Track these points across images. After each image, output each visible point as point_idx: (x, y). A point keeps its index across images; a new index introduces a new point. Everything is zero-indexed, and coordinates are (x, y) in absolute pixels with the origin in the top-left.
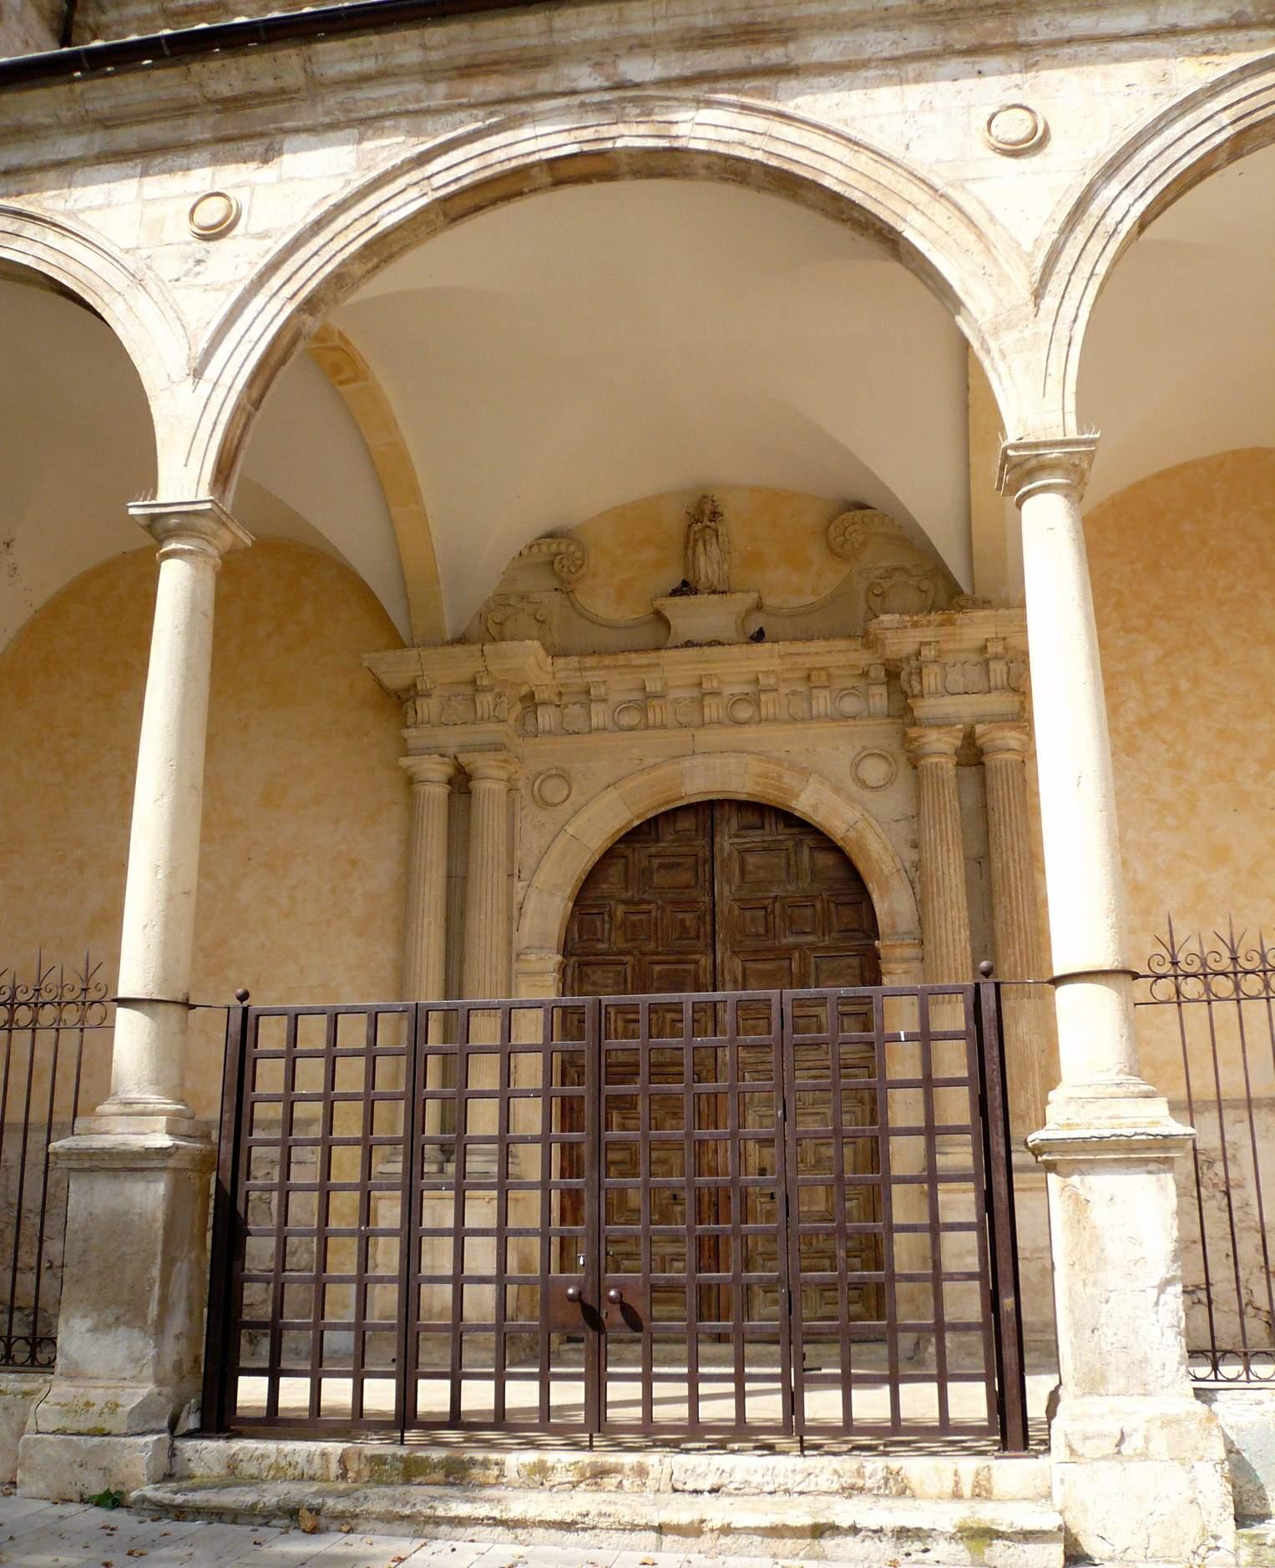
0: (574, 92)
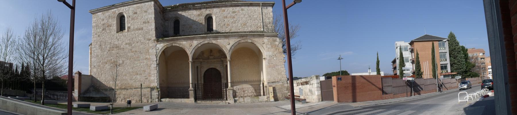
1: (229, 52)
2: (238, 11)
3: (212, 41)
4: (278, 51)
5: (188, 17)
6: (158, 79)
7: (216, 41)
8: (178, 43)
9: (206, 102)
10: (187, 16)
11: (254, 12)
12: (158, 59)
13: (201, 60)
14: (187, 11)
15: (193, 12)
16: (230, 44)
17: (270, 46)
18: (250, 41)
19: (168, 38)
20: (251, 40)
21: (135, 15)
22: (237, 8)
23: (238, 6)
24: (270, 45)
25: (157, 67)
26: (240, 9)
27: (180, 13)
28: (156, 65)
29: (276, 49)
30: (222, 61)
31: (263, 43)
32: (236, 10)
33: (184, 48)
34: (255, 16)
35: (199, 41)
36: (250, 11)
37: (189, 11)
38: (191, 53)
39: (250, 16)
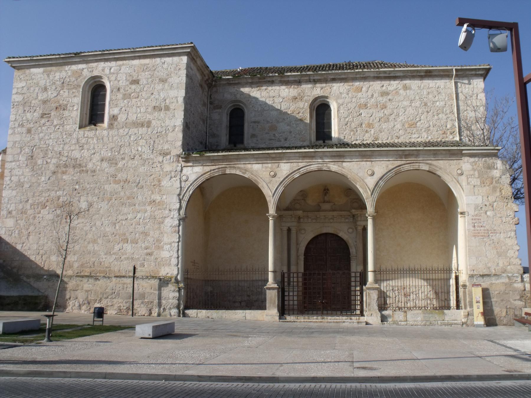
1: (372, 194)
2: (394, 92)
3: (328, 165)
4: (498, 194)
5: (266, 104)
6: (180, 259)
7: (339, 166)
8: (239, 168)
9: (309, 319)
10: (263, 99)
11: (435, 93)
12: (184, 204)
13: (300, 213)
14: (264, 88)
15: (280, 90)
16: (375, 175)
17: (479, 180)
18: (425, 167)
19: (216, 154)
20: (428, 164)
22: (392, 82)
23: (395, 78)
24: (478, 178)
25: (181, 228)
26: (400, 86)
27: (246, 90)
28: (177, 222)
29: (494, 189)
30: (354, 216)
31: (459, 172)
32: (390, 88)
33: (255, 180)
34: (438, 103)
35: (295, 164)
36: (425, 91)
37: (270, 88)
38: (273, 197)
39: (426, 104)
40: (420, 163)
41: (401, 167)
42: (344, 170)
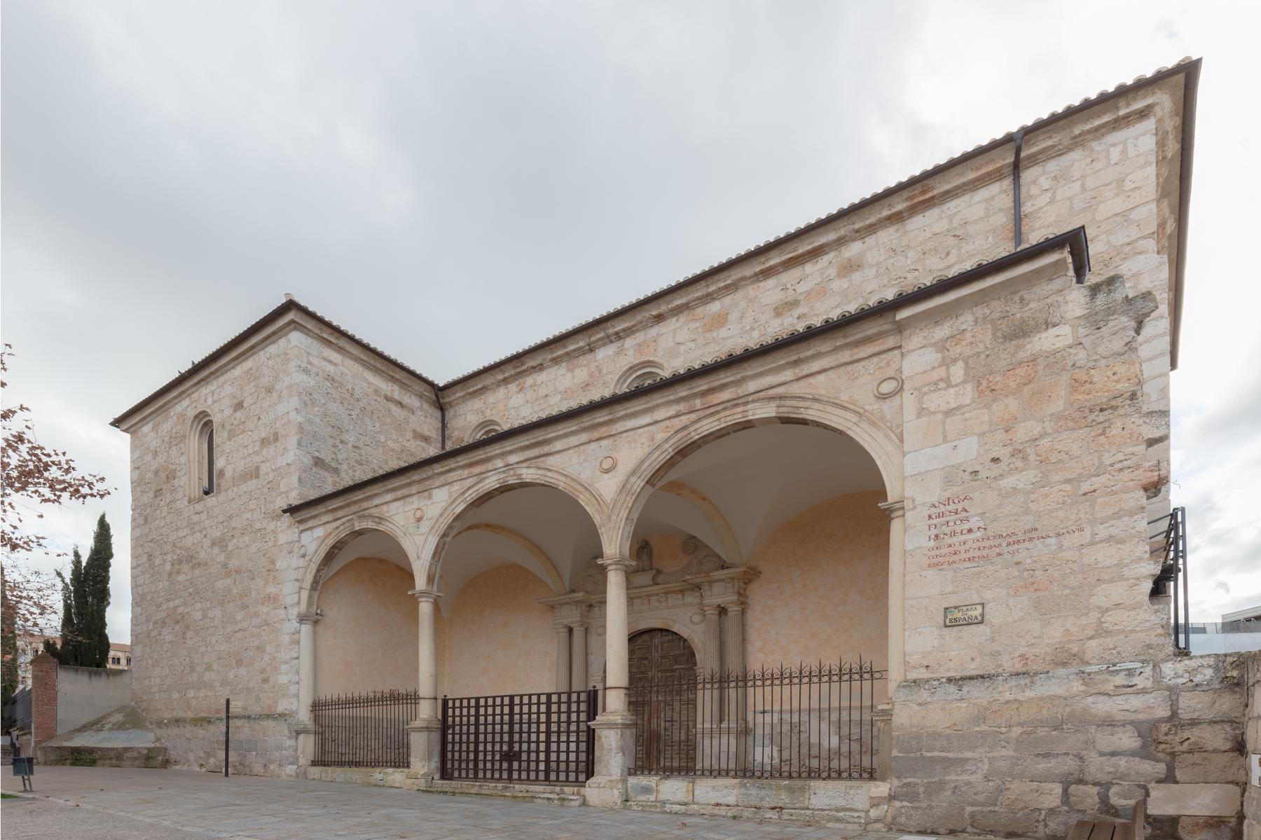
0: (496, 469)
7: (539, 468)
16: (620, 467)
21: (238, 414)
40: (746, 403)
41: (692, 429)
42: (550, 474)
